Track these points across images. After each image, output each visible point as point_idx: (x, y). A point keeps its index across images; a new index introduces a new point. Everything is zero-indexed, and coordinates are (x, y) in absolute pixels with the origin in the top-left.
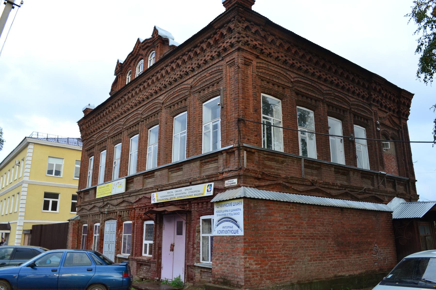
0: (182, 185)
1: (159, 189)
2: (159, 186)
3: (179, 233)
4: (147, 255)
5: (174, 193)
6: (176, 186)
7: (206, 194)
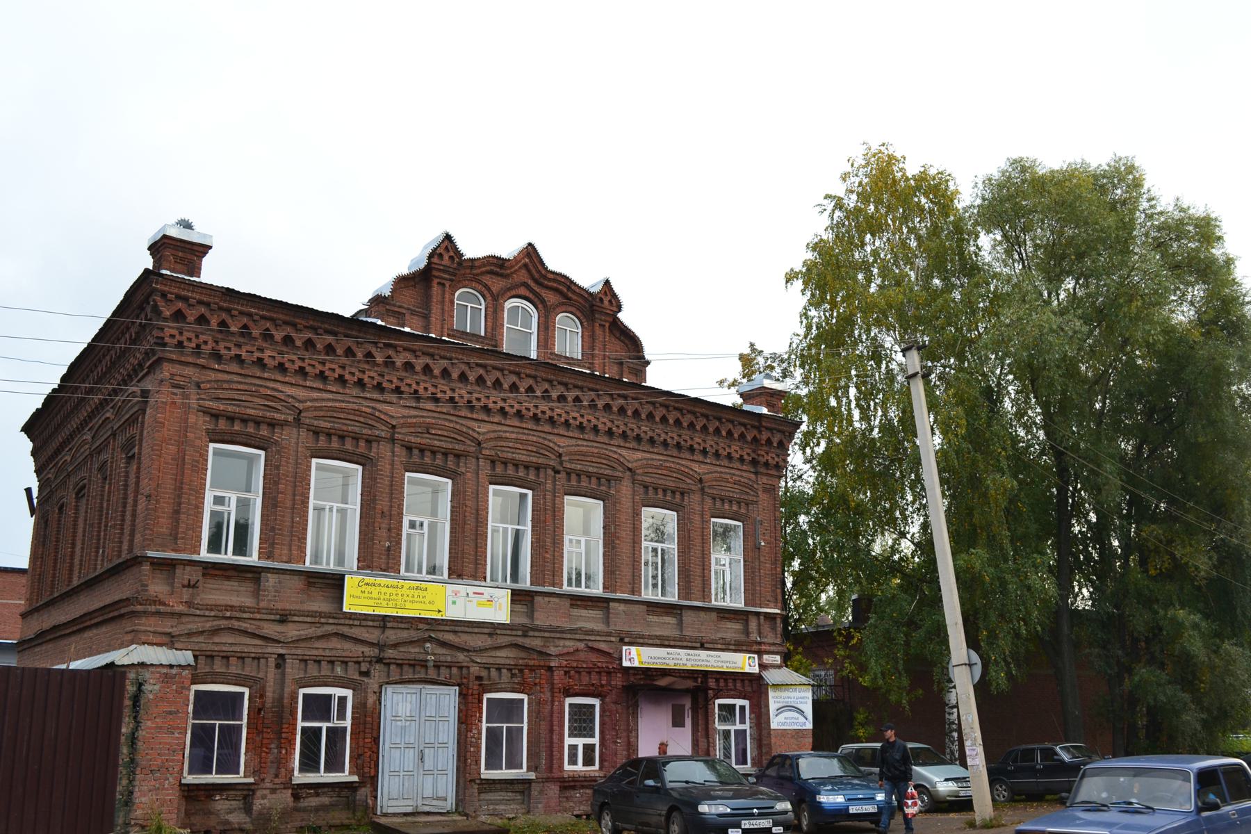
0: (685, 644)
1: (627, 640)
2: (629, 634)
3: (678, 722)
4: (580, 767)
5: (684, 658)
6: (672, 643)
7: (747, 670)
